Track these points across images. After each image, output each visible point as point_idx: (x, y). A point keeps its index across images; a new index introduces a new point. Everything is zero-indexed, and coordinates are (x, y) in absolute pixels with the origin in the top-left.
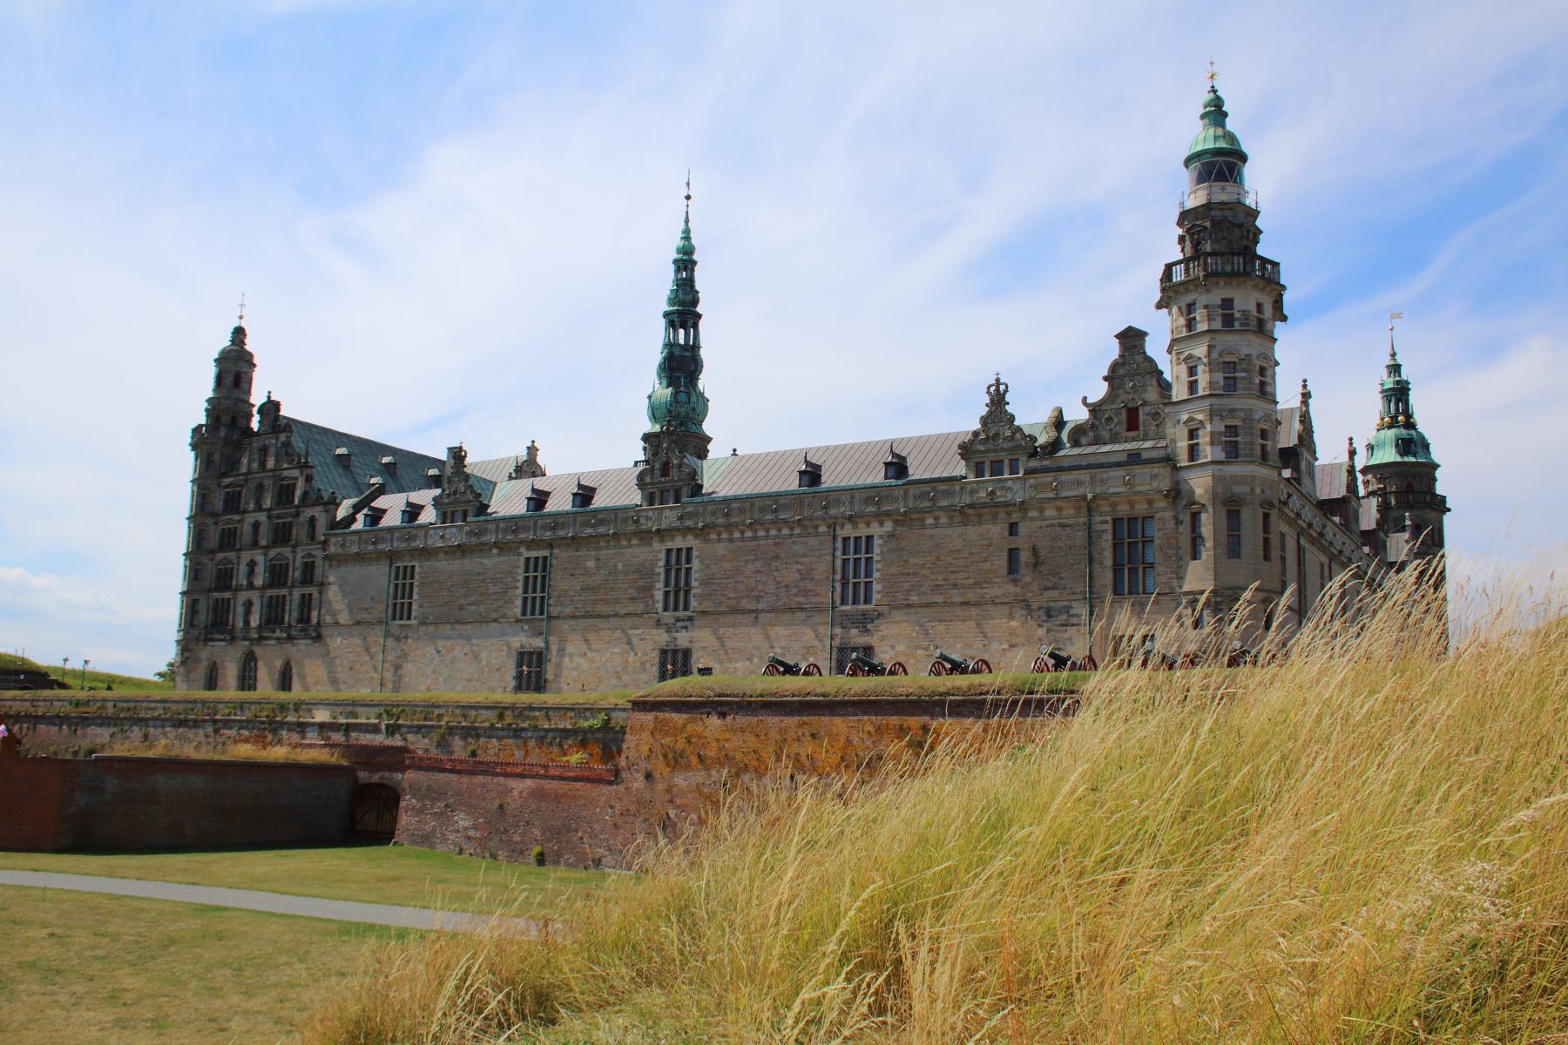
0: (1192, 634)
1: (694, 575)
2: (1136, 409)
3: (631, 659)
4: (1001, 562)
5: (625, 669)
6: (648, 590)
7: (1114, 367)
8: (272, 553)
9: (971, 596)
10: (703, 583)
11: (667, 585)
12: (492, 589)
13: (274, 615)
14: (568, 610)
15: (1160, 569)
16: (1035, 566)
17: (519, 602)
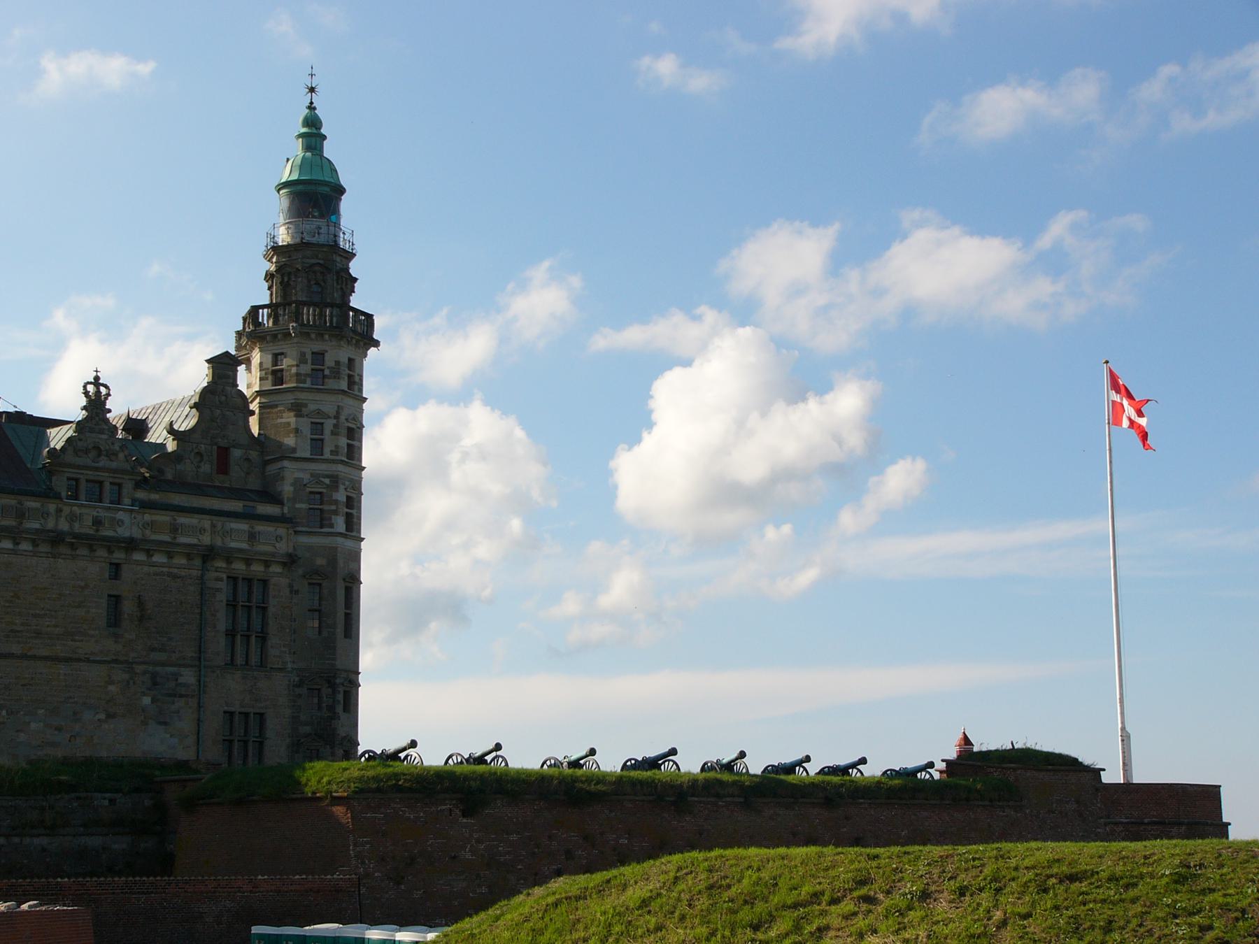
2: (227, 449)
7: (205, 392)
16: (141, 619)
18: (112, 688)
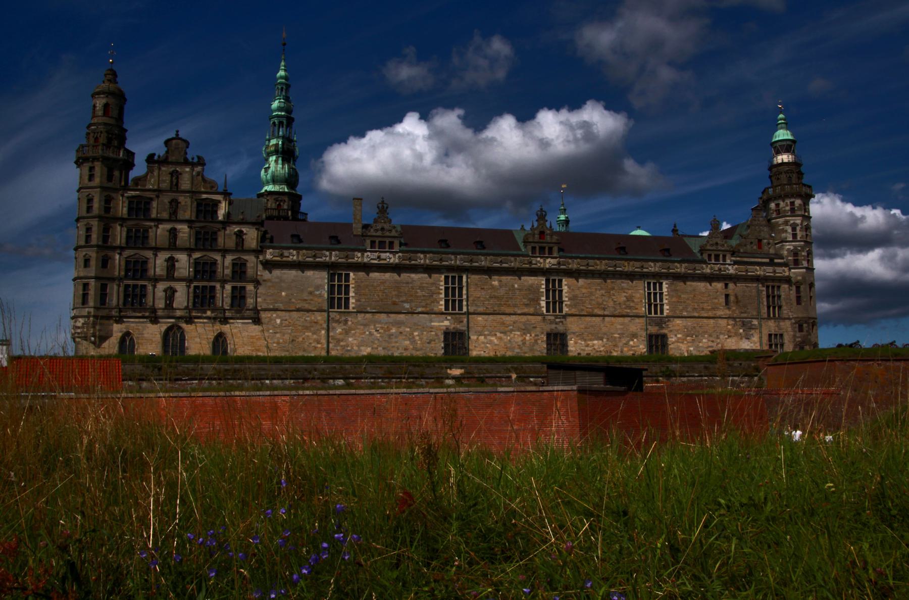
0: (798, 334)
1: (564, 294)
3: (527, 338)
4: (722, 300)
5: (524, 344)
6: (537, 301)
8: (197, 255)
9: (710, 314)
10: (570, 299)
11: (548, 297)
12: (420, 293)
13: (203, 300)
14: (481, 309)
15: (784, 308)
17: (443, 302)
18: (729, 327)
